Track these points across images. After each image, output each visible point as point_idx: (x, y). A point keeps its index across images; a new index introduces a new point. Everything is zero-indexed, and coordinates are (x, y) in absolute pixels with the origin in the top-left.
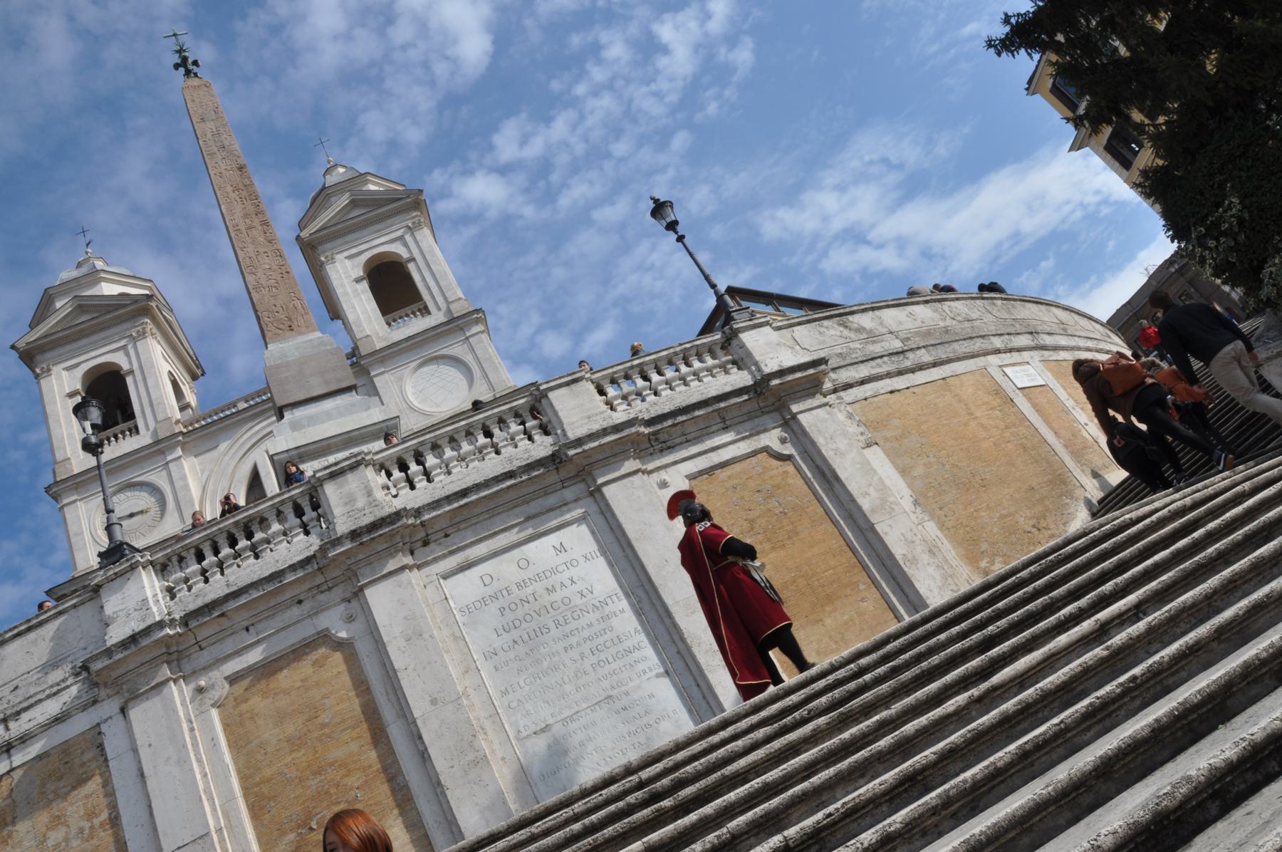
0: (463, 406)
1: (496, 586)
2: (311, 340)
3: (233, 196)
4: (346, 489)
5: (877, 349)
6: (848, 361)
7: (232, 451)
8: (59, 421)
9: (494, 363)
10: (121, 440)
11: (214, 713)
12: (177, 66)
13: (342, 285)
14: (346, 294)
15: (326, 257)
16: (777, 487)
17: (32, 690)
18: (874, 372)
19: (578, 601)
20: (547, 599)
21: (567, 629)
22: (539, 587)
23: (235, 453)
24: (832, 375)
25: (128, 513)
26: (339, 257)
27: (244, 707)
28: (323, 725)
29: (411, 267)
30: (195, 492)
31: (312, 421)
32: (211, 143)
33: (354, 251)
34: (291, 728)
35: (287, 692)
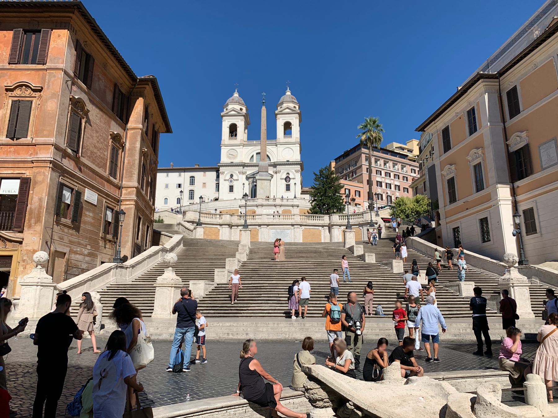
5: (306, 204)
26: (281, 119)
29: (293, 127)
31: (262, 176)
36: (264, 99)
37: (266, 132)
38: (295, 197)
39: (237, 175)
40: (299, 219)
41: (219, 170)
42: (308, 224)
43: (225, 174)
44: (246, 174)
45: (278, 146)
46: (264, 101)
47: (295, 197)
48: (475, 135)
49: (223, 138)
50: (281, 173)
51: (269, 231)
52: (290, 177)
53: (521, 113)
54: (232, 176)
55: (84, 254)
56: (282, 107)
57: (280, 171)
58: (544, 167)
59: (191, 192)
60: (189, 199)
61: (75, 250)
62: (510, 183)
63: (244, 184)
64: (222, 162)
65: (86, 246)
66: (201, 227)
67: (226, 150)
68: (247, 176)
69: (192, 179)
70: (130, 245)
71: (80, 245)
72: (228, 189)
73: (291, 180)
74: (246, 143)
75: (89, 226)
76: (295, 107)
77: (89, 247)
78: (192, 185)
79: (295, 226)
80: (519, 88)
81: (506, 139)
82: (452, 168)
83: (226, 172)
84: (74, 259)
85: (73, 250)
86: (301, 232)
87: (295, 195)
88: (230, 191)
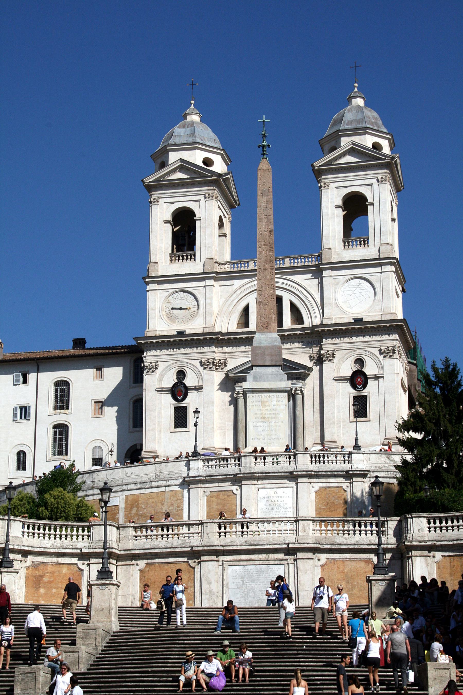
0: (363, 314)
1: (268, 495)
2: (273, 338)
3: (263, 247)
4: (246, 461)
6: (380, 470)
7: (239, 292)
8: (156, 237)
9: (389, 294)
10: (185, 260)
11: (206, 497)
12: (260, 146)
13: (327, 208)
14: (328, 215)
15: (325, 184)
16: (339, 497)
17: (172, 476)
18: (385, 476)
19: (282, 505)
20: (277, 502)
21: (278, 510)
22: (276, 499)
23: (240, 293)
24: (372, 473)
25: (179, 307)
26: (332, 185)
27: (212, 499)
28: (225, 509)
29: (370, 208)
30: (215, 309)
32: (262, 211)
33: (341, 184)
34: (219, 507)
35: (221, 499)
36: (264, 136)
37: (272, 241)
38: (357, 447)
39: (200, 377)
40: (311, 532)
42: (338, 547)
43: (158, 371)
44: (229, 367)
45: (325, 273)
46: (265, 143)
47: (357, 447)
49: (153, 259)
50: (335, 360)
51: (223, 570)
52: (367, 374)
54: (181, 374)
56: (333, 149)
57: (333, 356)
59: (58, 430)
60: (54, 454)
63: (196, 412)
64: (150, 334)
66: (9, 570)
67: (166, 294)
68: (227, 374)
69: (62, 390)
73: (371, 383)
74: (227, 268)
76: (376, 146)
78: (62, 408)
79: (300, 555)
83: (161, 366)
86: (319, 570)
87: (356, 440)
88: (176, 426)
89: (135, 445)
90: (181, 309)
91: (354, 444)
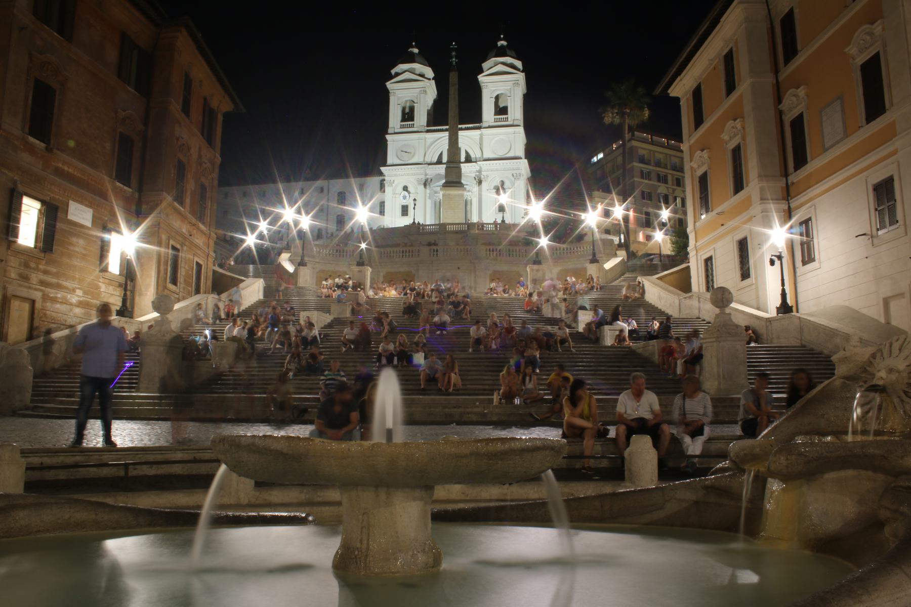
41: (384, 180)
48: (734, 96)
50: (489, 180)
53: (800, 54)
55: (70, 302)
58: (827, 145)
61: (51, 295)
62: (781, 176)
65: (74, 290)
66: (305, 267)
70: (153, 290)
71: (61, 288)
72: (399, 211)
75: (78, 260)
77: (79, 292)
80: (796, 11)
81: (779, 100)
82: (704, 156)
84: (51, 309)
85: (49, 296)
89: (380, 226)
90: (406, 152)
91: (502, 219)
